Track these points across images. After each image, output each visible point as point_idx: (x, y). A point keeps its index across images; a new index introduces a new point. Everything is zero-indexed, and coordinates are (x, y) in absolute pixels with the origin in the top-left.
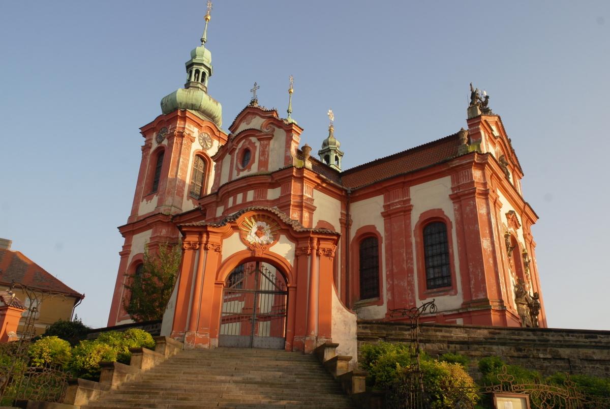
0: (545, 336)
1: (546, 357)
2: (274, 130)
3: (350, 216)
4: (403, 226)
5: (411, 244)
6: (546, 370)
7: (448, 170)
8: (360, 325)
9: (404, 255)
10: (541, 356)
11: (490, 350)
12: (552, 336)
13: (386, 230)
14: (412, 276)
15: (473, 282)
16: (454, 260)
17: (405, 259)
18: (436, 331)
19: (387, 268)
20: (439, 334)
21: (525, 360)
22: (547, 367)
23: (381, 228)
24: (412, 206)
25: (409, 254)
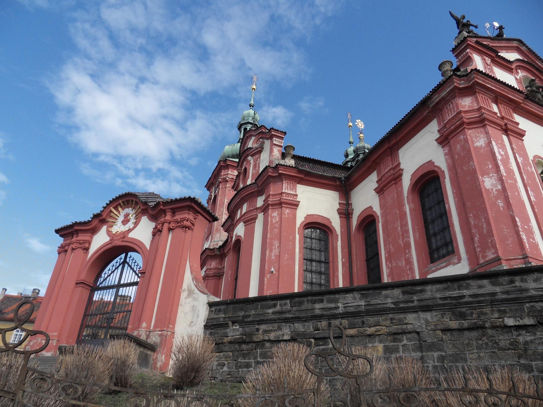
0: (517, 284)
1: (521, 323)
2: (263, 143)
3: (351, 204)
4: (395, 195)
5: (405, 213)
6: (526, 350)
7: (430, 112)
8: (213, 309)
9: (399, 228)
10: (510, 322)
11: (401, 322)
12: (535, 281)
13: (382, 207)
14: (410, 252)
15: (476, 239)
16: (451, 217)
17: (400, 233)
18: (314, 302)
19: (385, 249)
20: (318, 306)
21: (474, 334)
22: (526, 343)
23: (377, 209)
24: (402, 170)
25: (404, 225)
